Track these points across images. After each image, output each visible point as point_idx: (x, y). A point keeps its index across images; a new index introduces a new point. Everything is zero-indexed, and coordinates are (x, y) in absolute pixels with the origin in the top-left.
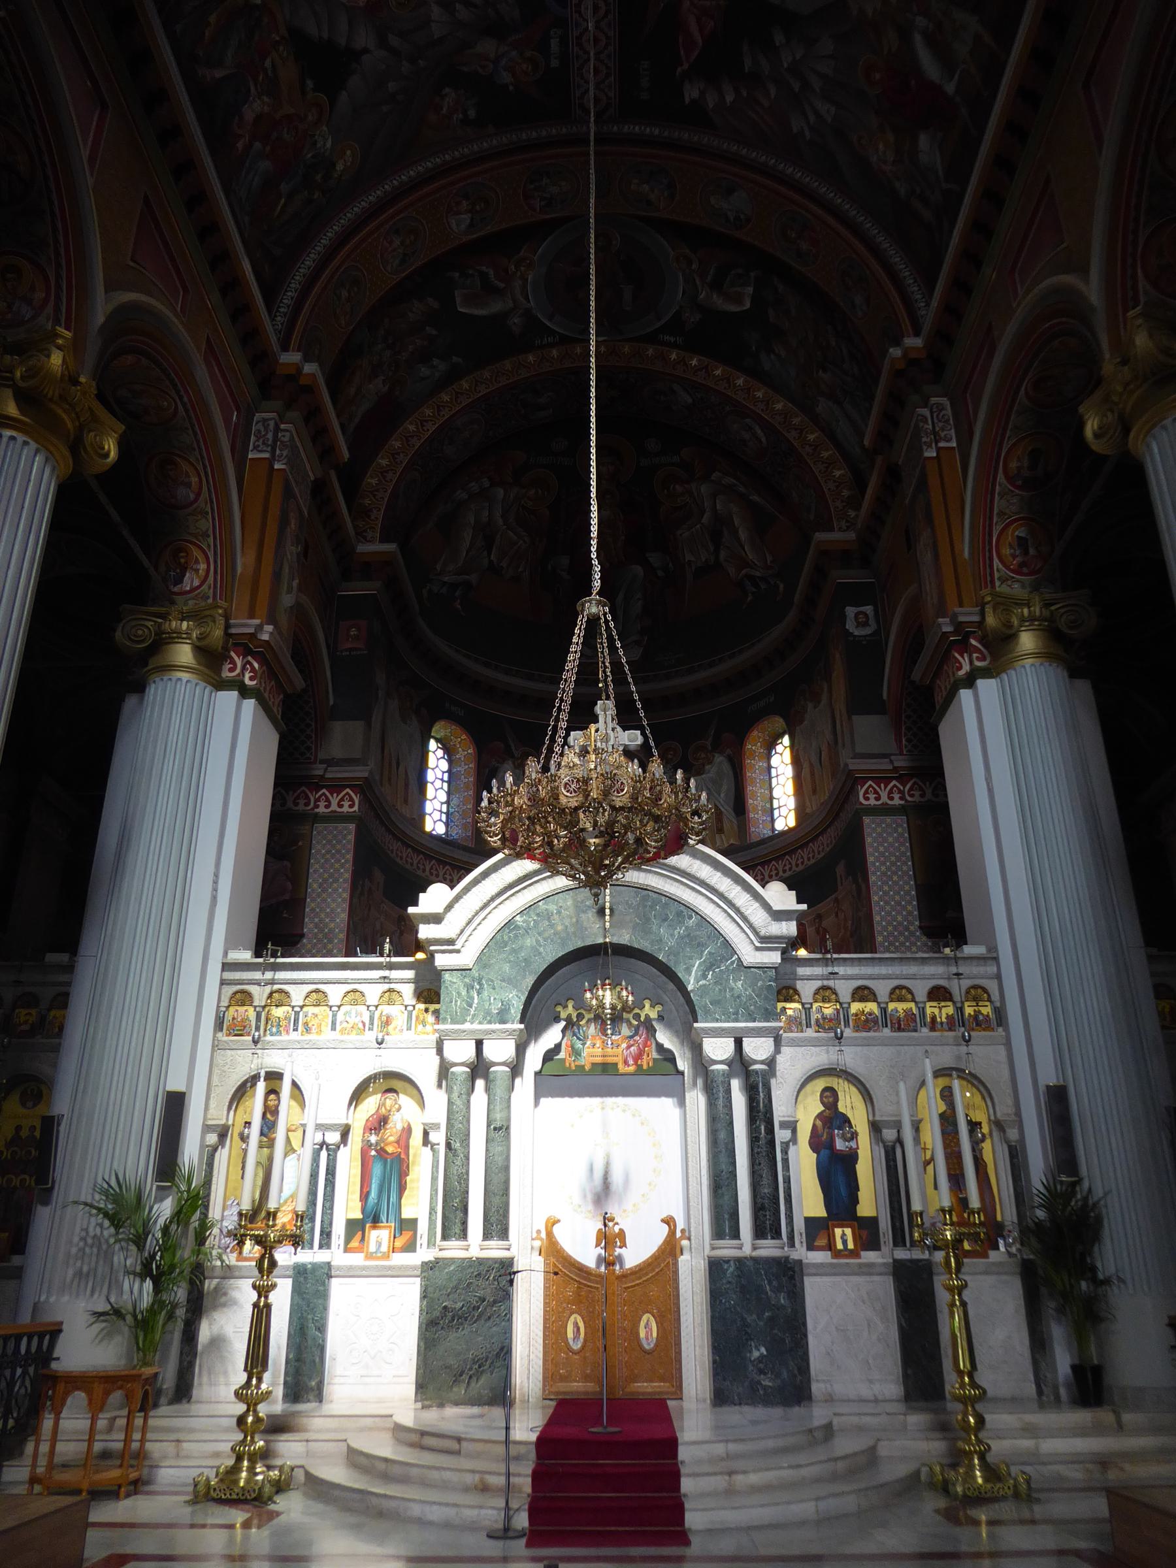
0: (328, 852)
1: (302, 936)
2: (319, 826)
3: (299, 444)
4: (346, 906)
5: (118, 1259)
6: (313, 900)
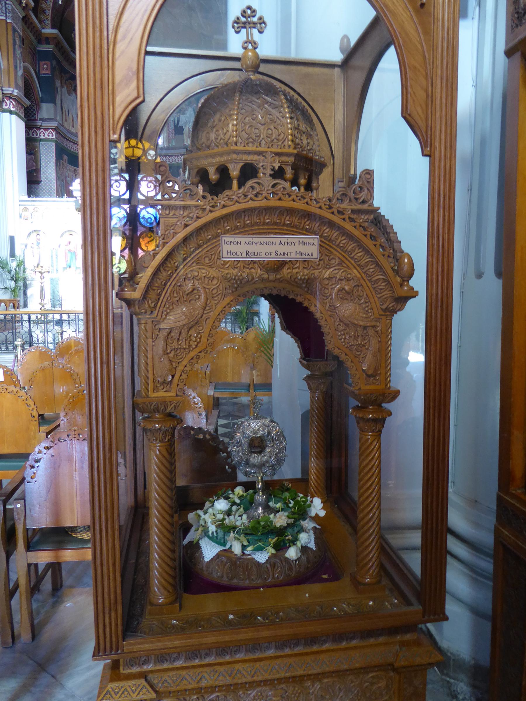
0: (46, 152)
1: (41, 181)
2: (42, 143)
3: (14, 7)
4: (55, 171)
5: (4, 276)
6: (43, 169)
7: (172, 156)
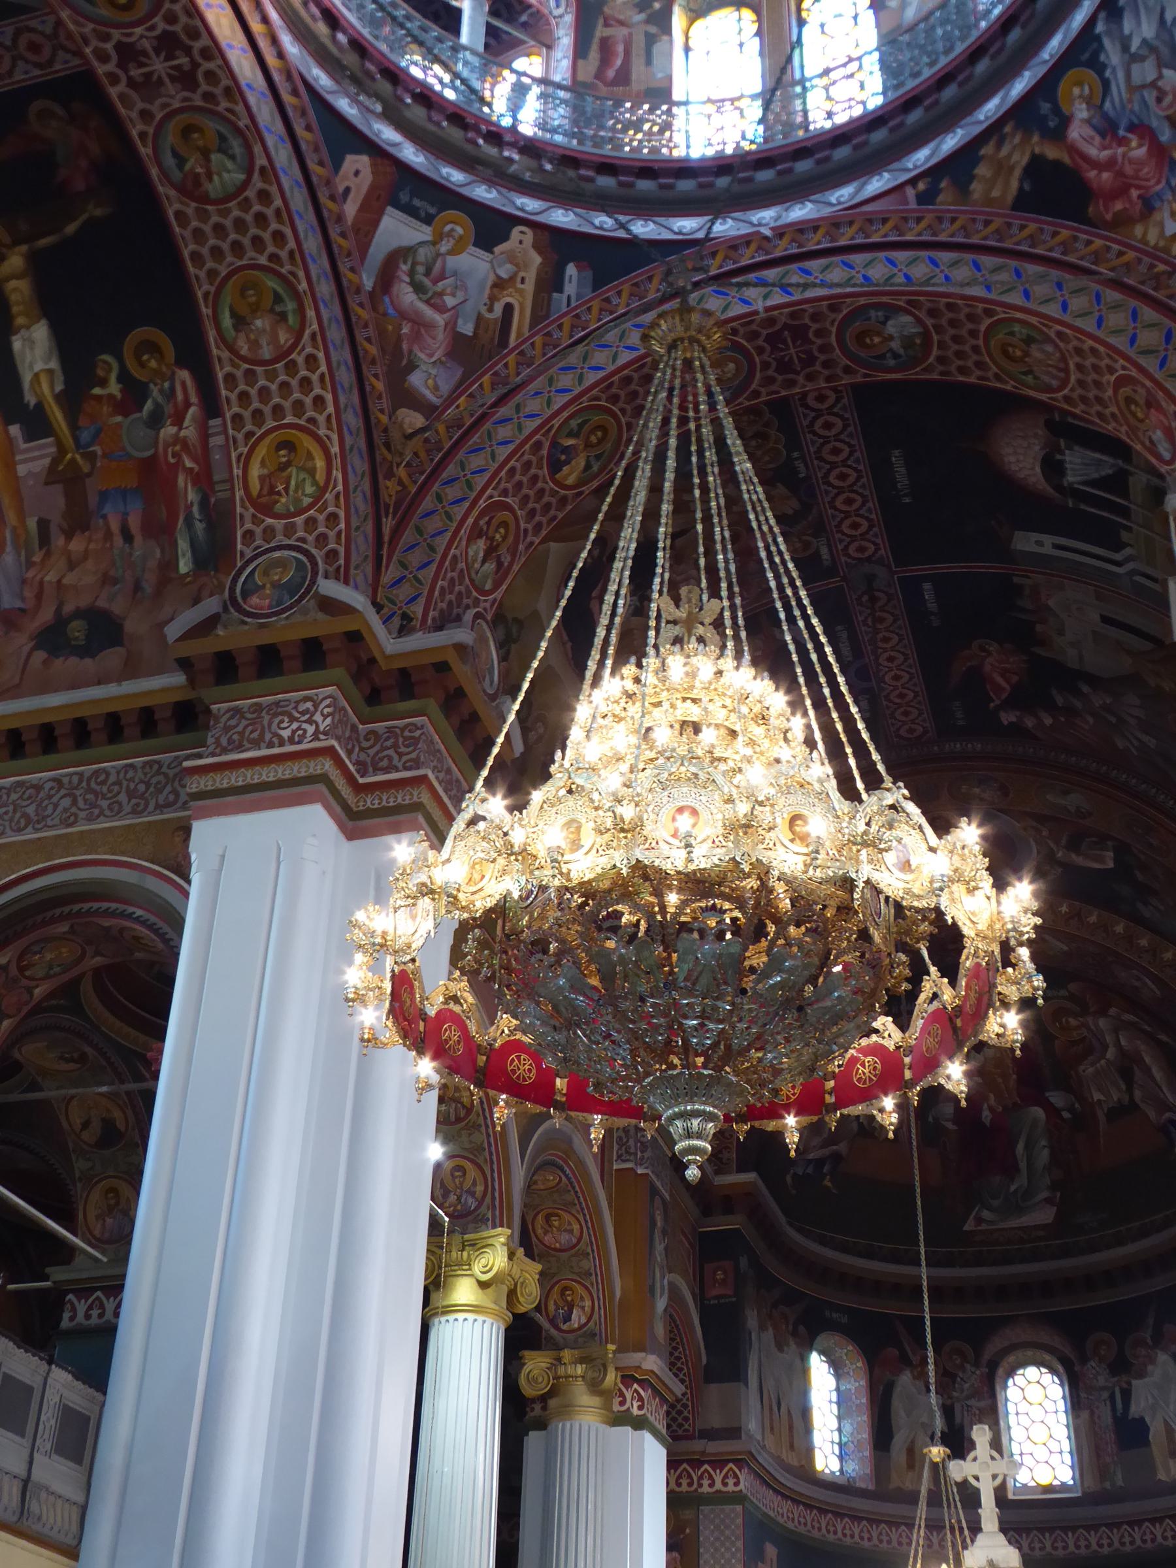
7: (1139, 1523)
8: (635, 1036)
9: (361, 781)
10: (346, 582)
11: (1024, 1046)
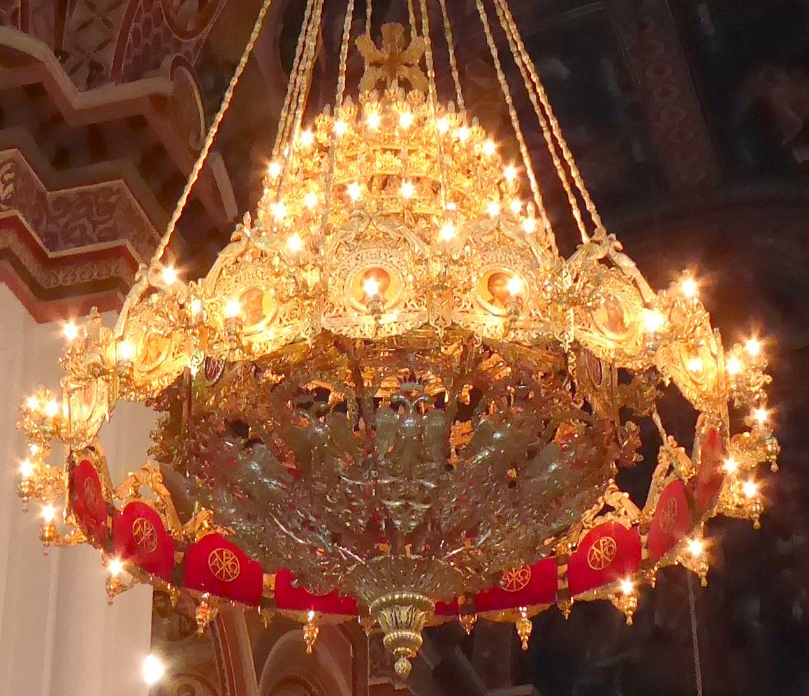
8: (333, 520)
9: (51, 255)
10: (25, 29)
11: (763, 517)
